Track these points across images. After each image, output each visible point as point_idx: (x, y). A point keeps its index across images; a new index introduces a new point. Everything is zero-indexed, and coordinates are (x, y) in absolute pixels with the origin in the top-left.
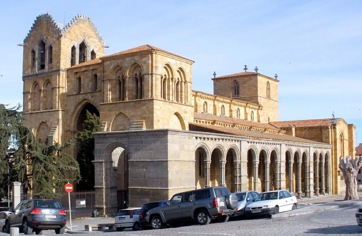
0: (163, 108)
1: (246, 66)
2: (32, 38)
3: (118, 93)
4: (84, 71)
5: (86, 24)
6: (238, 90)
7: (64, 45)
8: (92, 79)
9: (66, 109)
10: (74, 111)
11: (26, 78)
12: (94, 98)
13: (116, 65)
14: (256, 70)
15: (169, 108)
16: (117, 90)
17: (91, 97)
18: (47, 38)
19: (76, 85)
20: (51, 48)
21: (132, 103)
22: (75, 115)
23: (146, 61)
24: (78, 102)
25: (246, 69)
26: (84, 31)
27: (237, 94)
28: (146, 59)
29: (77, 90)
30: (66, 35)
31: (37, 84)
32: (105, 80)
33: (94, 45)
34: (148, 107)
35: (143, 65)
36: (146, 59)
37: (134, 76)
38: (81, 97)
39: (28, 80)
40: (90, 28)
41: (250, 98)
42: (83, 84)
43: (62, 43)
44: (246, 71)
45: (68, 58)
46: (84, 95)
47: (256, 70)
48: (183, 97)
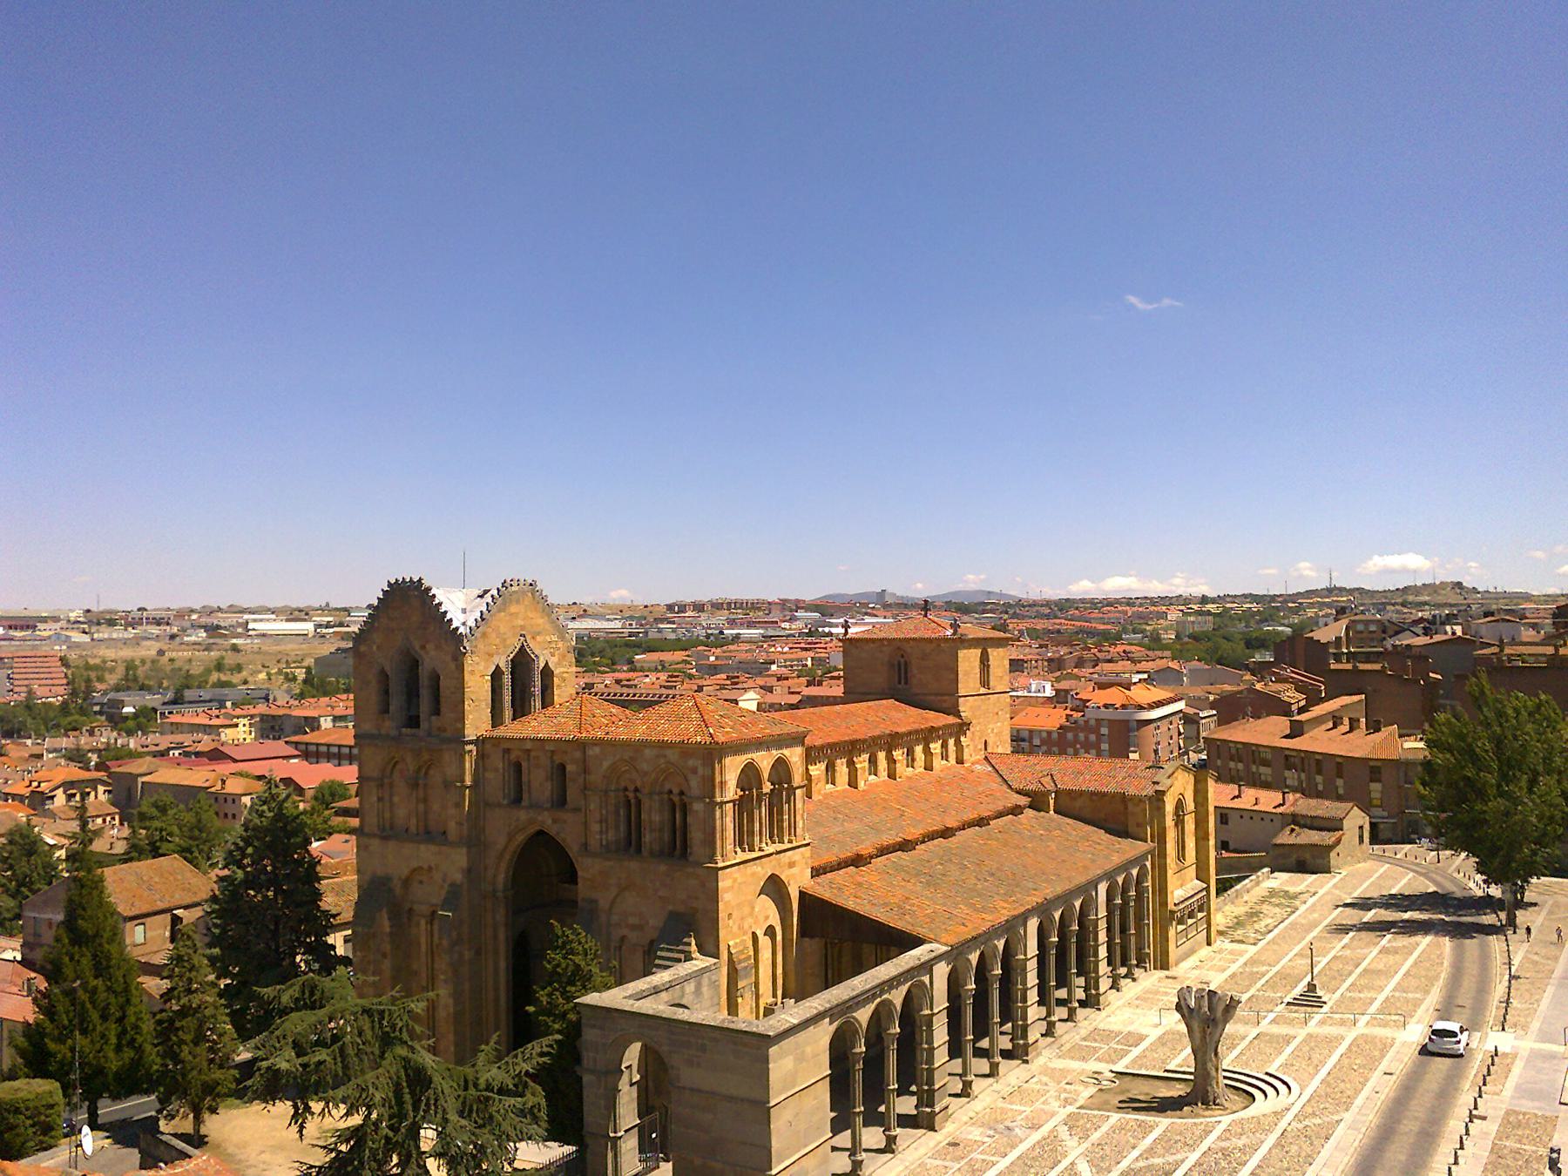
0: (739, 881)
2: (377, 637)
3: (622, 828)
4: (529, 751)
5: (526, 603)
6: (906, 673)
7: (472, 672)
8: (552, 774)
9: (482, 838)
10: (506, 847)
15: (753, 874)
16: (622, 819)
17: (550, 821)
18: (423, 647)
19: (509, 781)
20: (435, 679)
21: (663, 868)
22: (507, 857)
23: (696, 768)
26: (522, 623)
27: (903, 682)
29: (512, 793)
30: (476, 646)
31: (396, 763)
33: (549, 650)
37: (666, 796)
40: (536, 610)
41: (939, 698)
42: (529, 782)
43: (467, 668)
45: (483, 705)
48: (786, 824)
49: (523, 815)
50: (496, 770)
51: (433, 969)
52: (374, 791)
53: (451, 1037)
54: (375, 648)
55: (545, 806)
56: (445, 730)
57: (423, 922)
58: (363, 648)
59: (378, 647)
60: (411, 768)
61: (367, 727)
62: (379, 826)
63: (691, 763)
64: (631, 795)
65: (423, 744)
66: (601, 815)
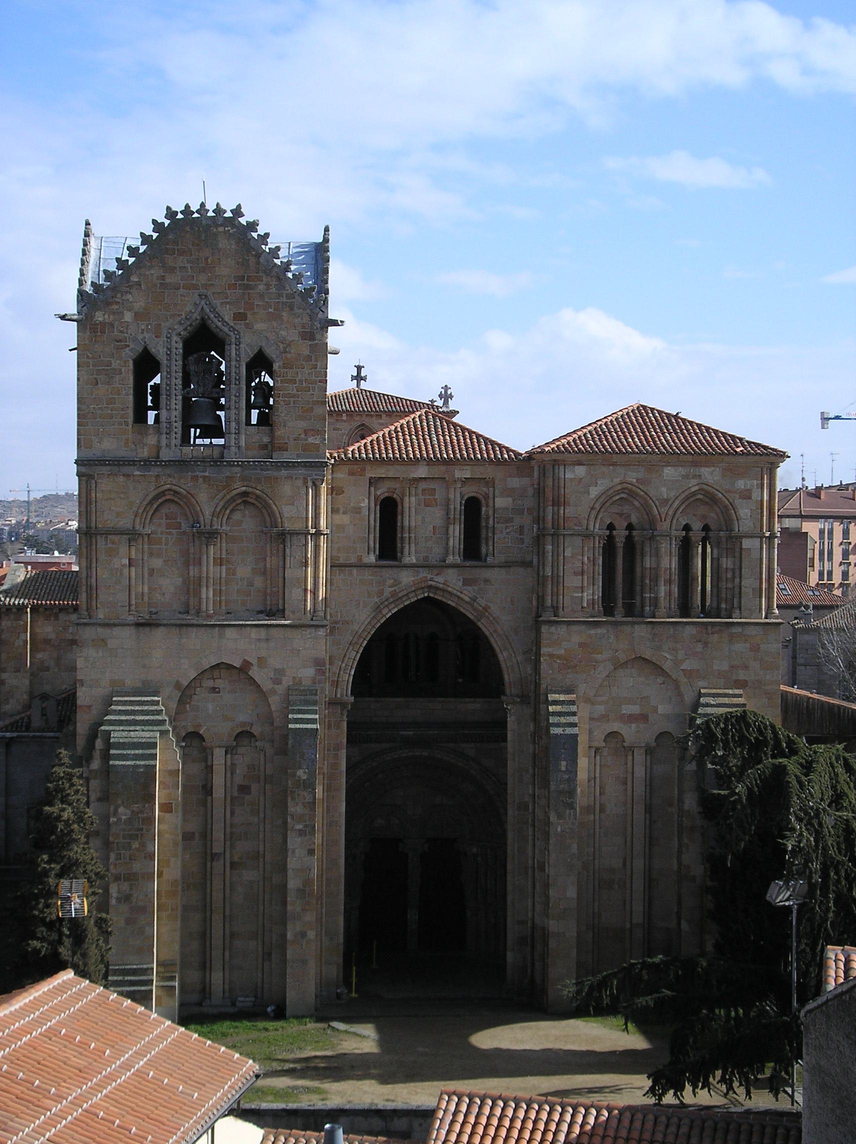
1: (359, 368)
2: (138, 300)
11: (105, 470)
12: (476, 588)
13: (619, 487)
14: (446, 396)
23: (749, 491)
24: (393, 594)
25: (359, 378)
28: (752, 485)
32: (564, 535)
34: (755, 649)
35: (738, 502)
36: (752, 485)
38: (407, 578)
39: (121, 479)
44: (358, 385)
46: (424, 574)
47: (446, 396)
49: (407, 578)
50: (357, 510)
51: (232, 826)
52: (123, 549)
53: (310, 917)
54: (128, 317)
55: (450, 559)
56: (283, 448)
57: (219, 753)
58: (99, 317)
59: (138, 316)
60: (208, 512)
61: (108, 446)
62: (130, 605)
63: (741, 484)
64: (620, 535)
65: (238, 469)
66: (583, 563)
